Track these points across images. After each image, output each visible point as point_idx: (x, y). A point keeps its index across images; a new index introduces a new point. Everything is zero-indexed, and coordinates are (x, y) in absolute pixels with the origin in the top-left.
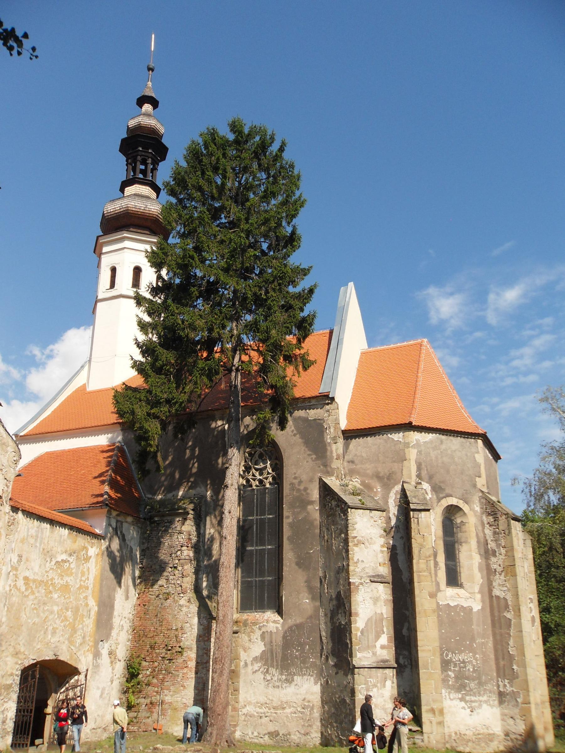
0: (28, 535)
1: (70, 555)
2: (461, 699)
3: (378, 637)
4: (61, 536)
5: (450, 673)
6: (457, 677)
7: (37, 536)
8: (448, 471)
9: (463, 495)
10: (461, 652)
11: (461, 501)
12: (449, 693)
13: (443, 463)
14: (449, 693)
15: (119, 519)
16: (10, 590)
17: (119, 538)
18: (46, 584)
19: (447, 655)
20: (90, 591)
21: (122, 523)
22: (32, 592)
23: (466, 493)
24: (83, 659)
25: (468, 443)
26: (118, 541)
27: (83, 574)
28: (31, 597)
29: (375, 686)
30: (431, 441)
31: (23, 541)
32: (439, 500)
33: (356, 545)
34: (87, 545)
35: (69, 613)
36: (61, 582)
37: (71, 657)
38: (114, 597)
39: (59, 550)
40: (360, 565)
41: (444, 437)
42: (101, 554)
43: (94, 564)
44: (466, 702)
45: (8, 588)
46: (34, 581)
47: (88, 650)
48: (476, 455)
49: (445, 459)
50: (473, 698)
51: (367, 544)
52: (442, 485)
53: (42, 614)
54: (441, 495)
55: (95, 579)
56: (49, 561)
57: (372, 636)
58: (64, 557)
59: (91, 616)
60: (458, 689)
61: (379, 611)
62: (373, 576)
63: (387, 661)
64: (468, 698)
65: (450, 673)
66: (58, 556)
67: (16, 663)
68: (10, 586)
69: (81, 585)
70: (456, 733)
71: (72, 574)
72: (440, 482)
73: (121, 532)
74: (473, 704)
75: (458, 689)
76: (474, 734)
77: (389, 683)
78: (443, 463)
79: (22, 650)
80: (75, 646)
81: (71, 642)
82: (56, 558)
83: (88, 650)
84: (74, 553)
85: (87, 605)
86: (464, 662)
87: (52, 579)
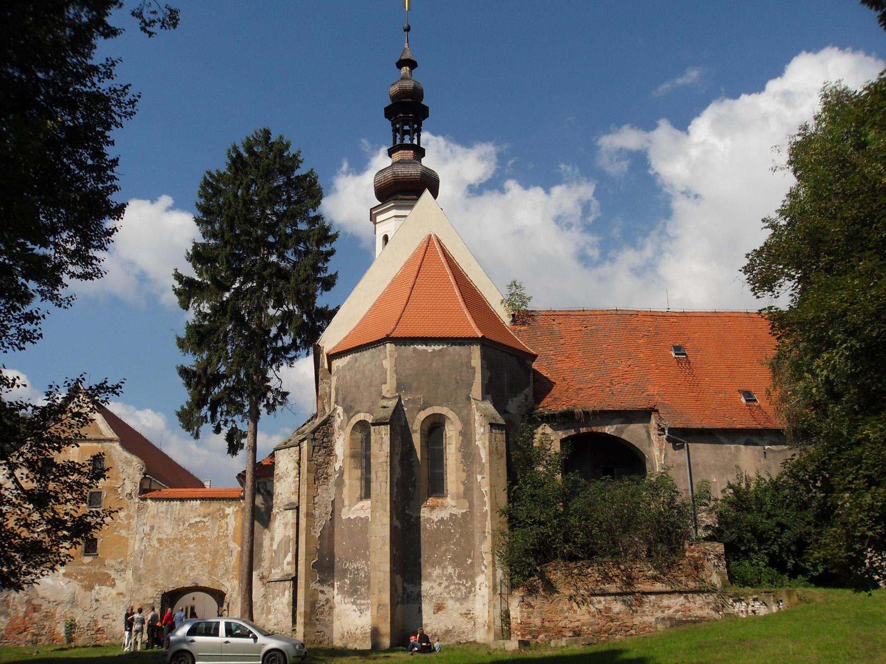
0: (158, 513)
1: (205, 517)
2: (354, 603)
3: (285, 556)
4: (192, 506)
5: (346, 580)
6: (351, 584)
7: (167, 511)
8: (358, 388)
9: (369, 408)
10: (356, 560)
11: (368, 414)
12: (345, 598)
13: (355, 381)
14: (345, 598)
15: (260, 481)
16: (145, 548)
17: (263, 495)
18: (180, 540)
19: (345, 565)
20: (230, 537)
21: (265, 483)
22: (167, 547)
23: (373, 405)
24: (228, 585)
25: (378, 352)
26: (261, 497)
27: (220, 527)
28: (166, 550)
29: (278, 595)
30: (348, 363)
31: (154, 517)
32: (349, 419)
33: (278, 481)
34: (222, 506)
35: (207, 556)
36: (197, 536)
37: (213, 584)
38: (262, 538)
39: (191, 515)
40: (280, 497)
41: (358, 355)
42: (240, 510)
43: (233, 519)
44: (357, 605)
45: (143, 547)
46: (167, 539)
47: (233, 578)
48: (384, 362)
49: (358, 377)
50: (363, 602)
51: (285, 478)
52: (352, 404)
53: (178, 559)
54: (351, 415)
55: (234, 529)
56: (182, 524)
57: (281, 555)
58: (198, 519)
59: (233, 554)
60: (351, 594)
61: (287, 534)
62: (288, 505)
63: (290, 575)
64: (358, 602)
65: (346, 580)
66: (191, 520)
67: (156, 591)
68: (145, 545)
69: (219, 535)
70: (348, 632)
71: (208, 529)
72: (351, 401)
73: (266, 490)
74: (362, 607)
75: (351, 594)
76: (361, 634)
77: (287, 592)
78: (355, 381)
79: (161, 582)
80: (217, 577)
81: (211, 573)
82: (188, 521)
83: (233, 578)
84: (209, 515)
85: (228, 547)
86: (357, 569)
87: (186, 536)
